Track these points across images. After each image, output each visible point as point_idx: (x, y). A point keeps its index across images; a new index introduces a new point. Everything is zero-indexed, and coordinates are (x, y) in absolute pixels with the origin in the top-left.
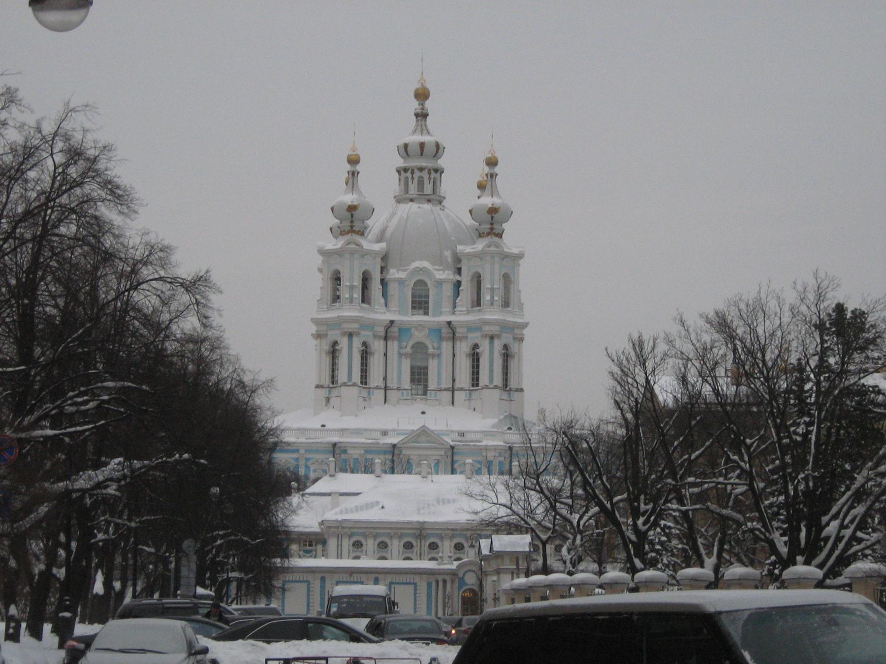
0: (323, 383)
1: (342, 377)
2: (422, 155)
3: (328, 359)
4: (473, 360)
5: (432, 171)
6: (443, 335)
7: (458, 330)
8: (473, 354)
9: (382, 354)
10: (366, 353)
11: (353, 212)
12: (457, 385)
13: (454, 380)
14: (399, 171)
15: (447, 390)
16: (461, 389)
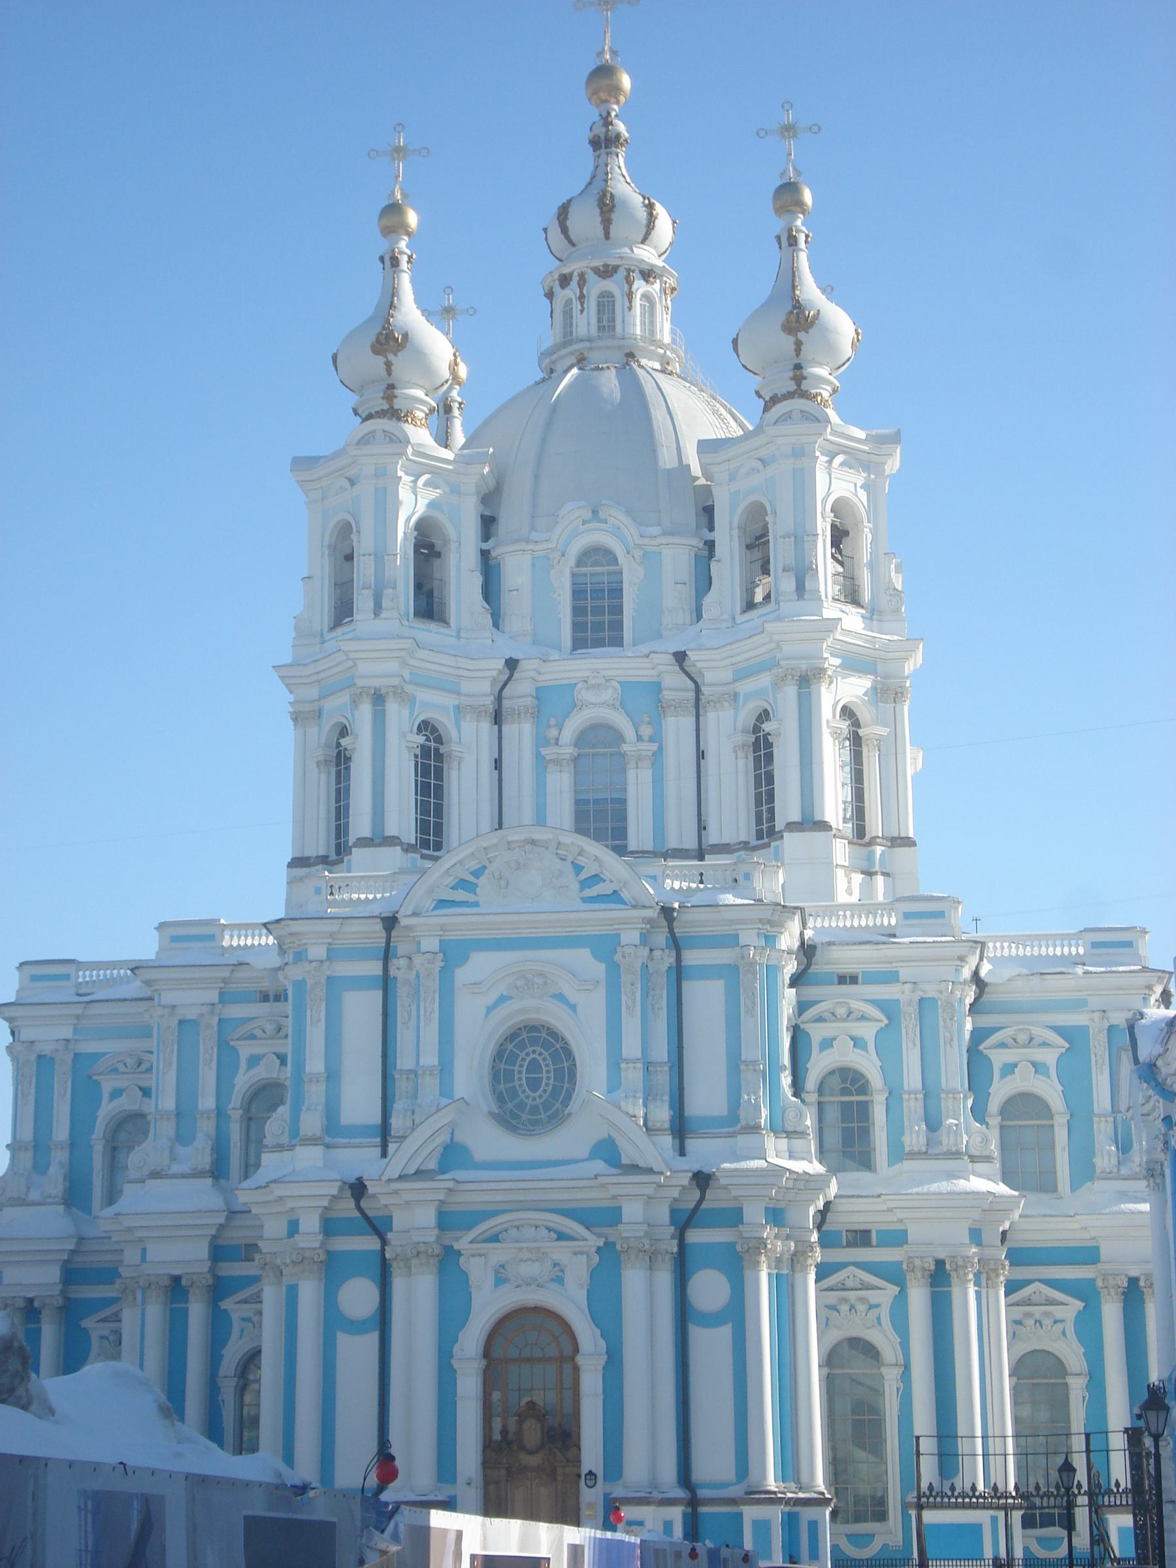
0: (311, 852)
1: (361, 825)
2: (607, 236)
3: (323, 777)
4: (757, 760)
5: (636, 275)
6: (667, 695)
7: (709, 677)
8: (756, 746)
10: (439, 757)
11: (391, 357)
12: (713, 837)
13: (702, 827)
14: (550, 295)
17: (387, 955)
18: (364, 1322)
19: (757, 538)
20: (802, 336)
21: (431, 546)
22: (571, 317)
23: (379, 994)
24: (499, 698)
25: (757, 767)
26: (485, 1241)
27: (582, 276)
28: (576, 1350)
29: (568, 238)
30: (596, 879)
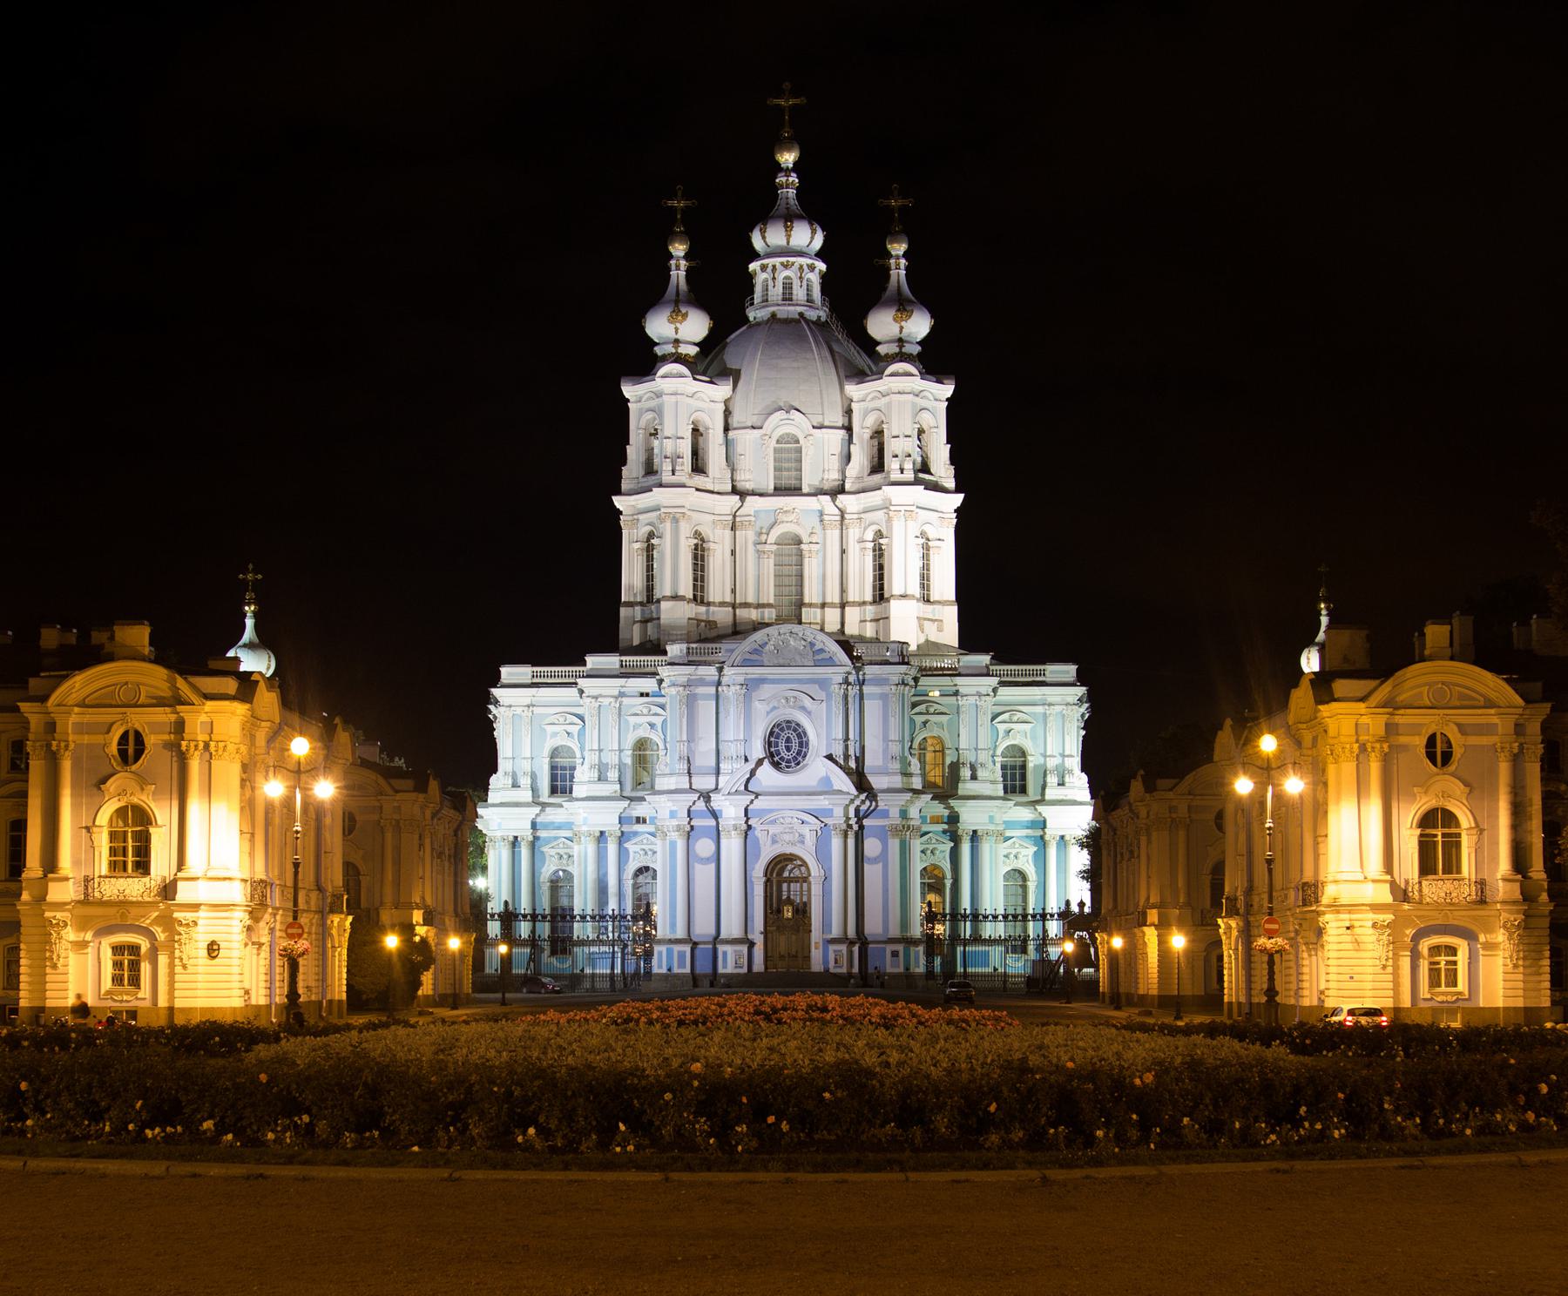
4: (875, 556)
8: (874, 550)
9: (728, 553)
10: (703, 550)
13: (843, 591)
15: (832, 605)
16: (854, 604)
17: (719, 683)
18: (708, 859)
19: (876, 432)
20: (903, 324)
21: (698, 430)
22: (767, 290)
23: (714, 702)
24: (735, 516)
25: (874, 561)
26: (767, 824)
27: (774, 266)
28: (810, 875)
29: (765, 241)
30: (822, 651)
